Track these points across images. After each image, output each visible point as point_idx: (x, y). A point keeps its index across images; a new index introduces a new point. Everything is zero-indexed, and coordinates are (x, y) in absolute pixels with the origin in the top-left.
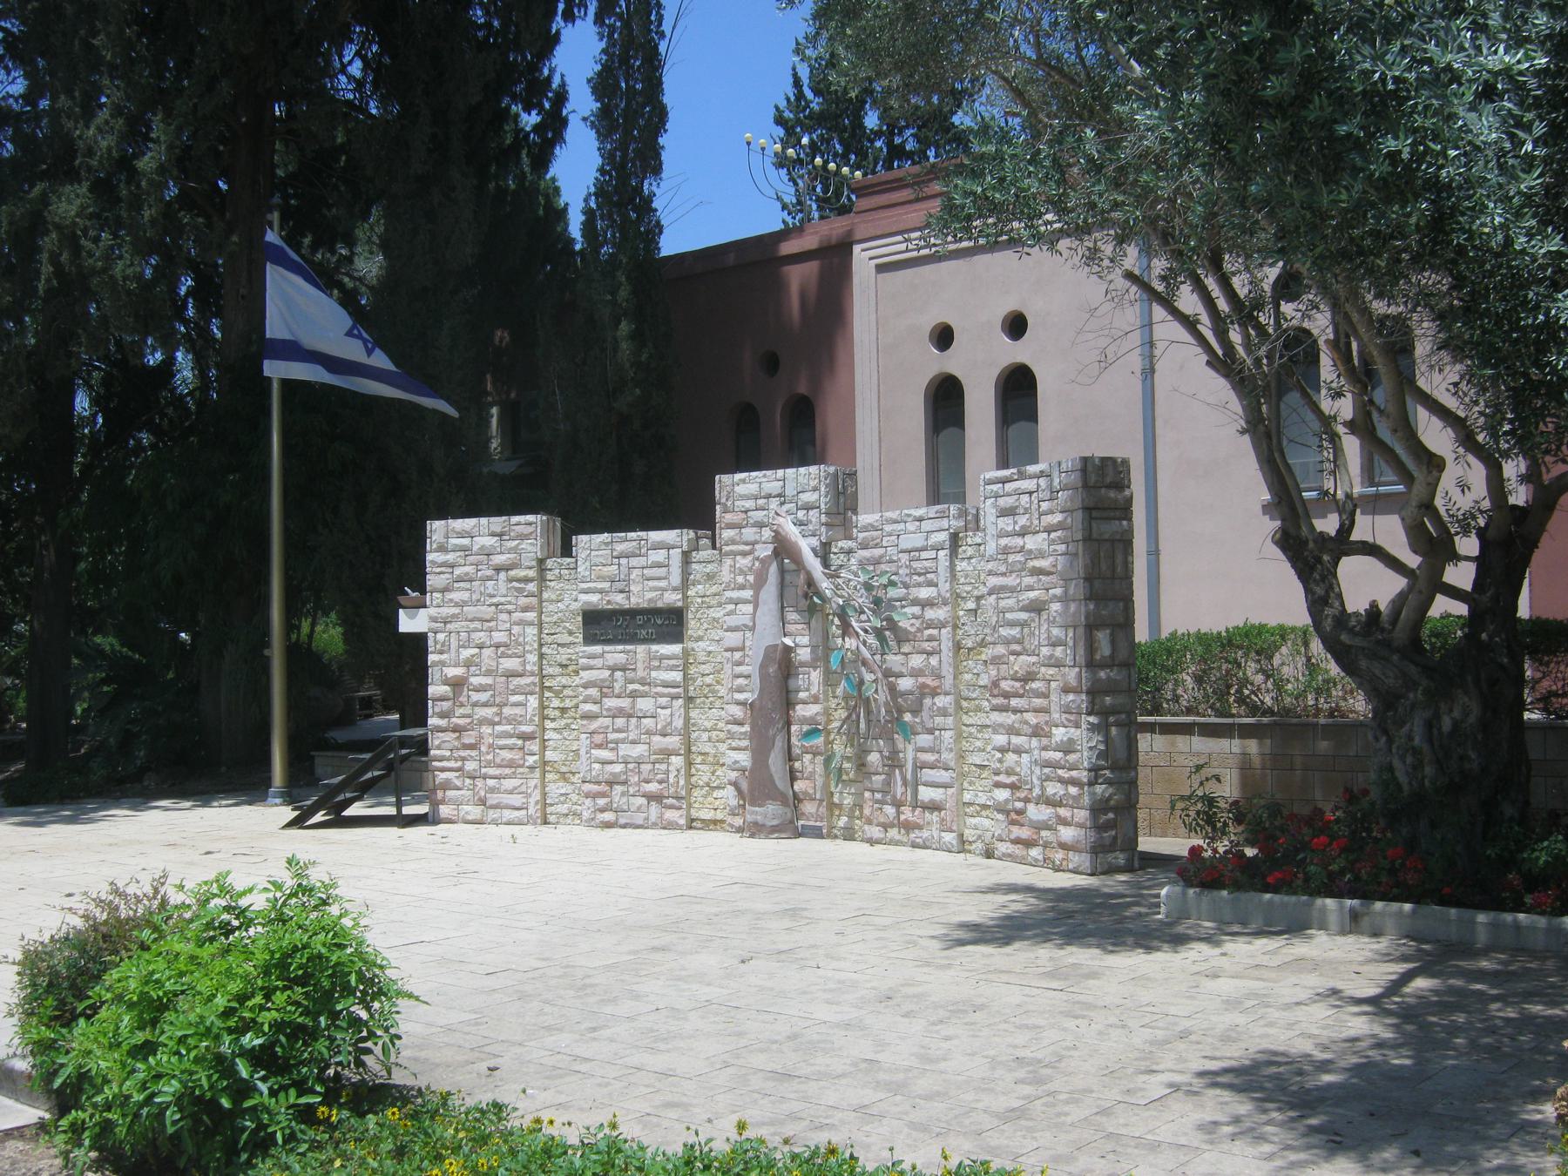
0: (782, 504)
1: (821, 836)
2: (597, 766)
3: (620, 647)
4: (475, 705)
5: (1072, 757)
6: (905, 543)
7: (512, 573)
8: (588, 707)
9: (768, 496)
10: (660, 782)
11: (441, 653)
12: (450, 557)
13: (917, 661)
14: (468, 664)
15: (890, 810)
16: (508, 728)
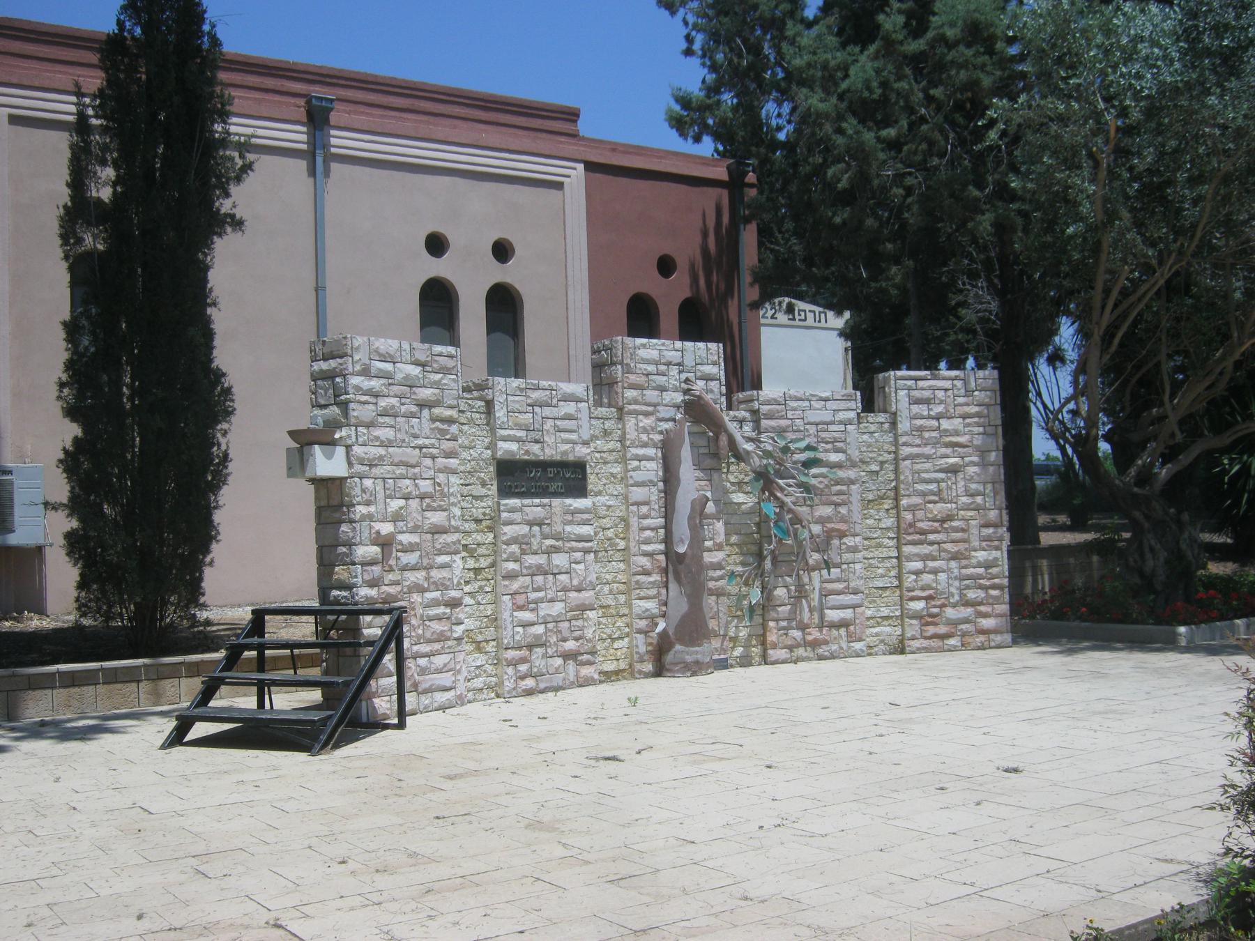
0: (680, 372)
1: (726, 667)
2: (520, 629)
3: (537, 501)
4: (404, 569)
5: (994, 570)
6: (812, 416)
7: (436, 411)
8: (511, 566)
9: (669, 364)
10: (576, 639)
11: (368, 503)
12: (375, 384)
13: (827, 511)
14: (396, 518)
15: (797, 634)
16: (437, 594)
